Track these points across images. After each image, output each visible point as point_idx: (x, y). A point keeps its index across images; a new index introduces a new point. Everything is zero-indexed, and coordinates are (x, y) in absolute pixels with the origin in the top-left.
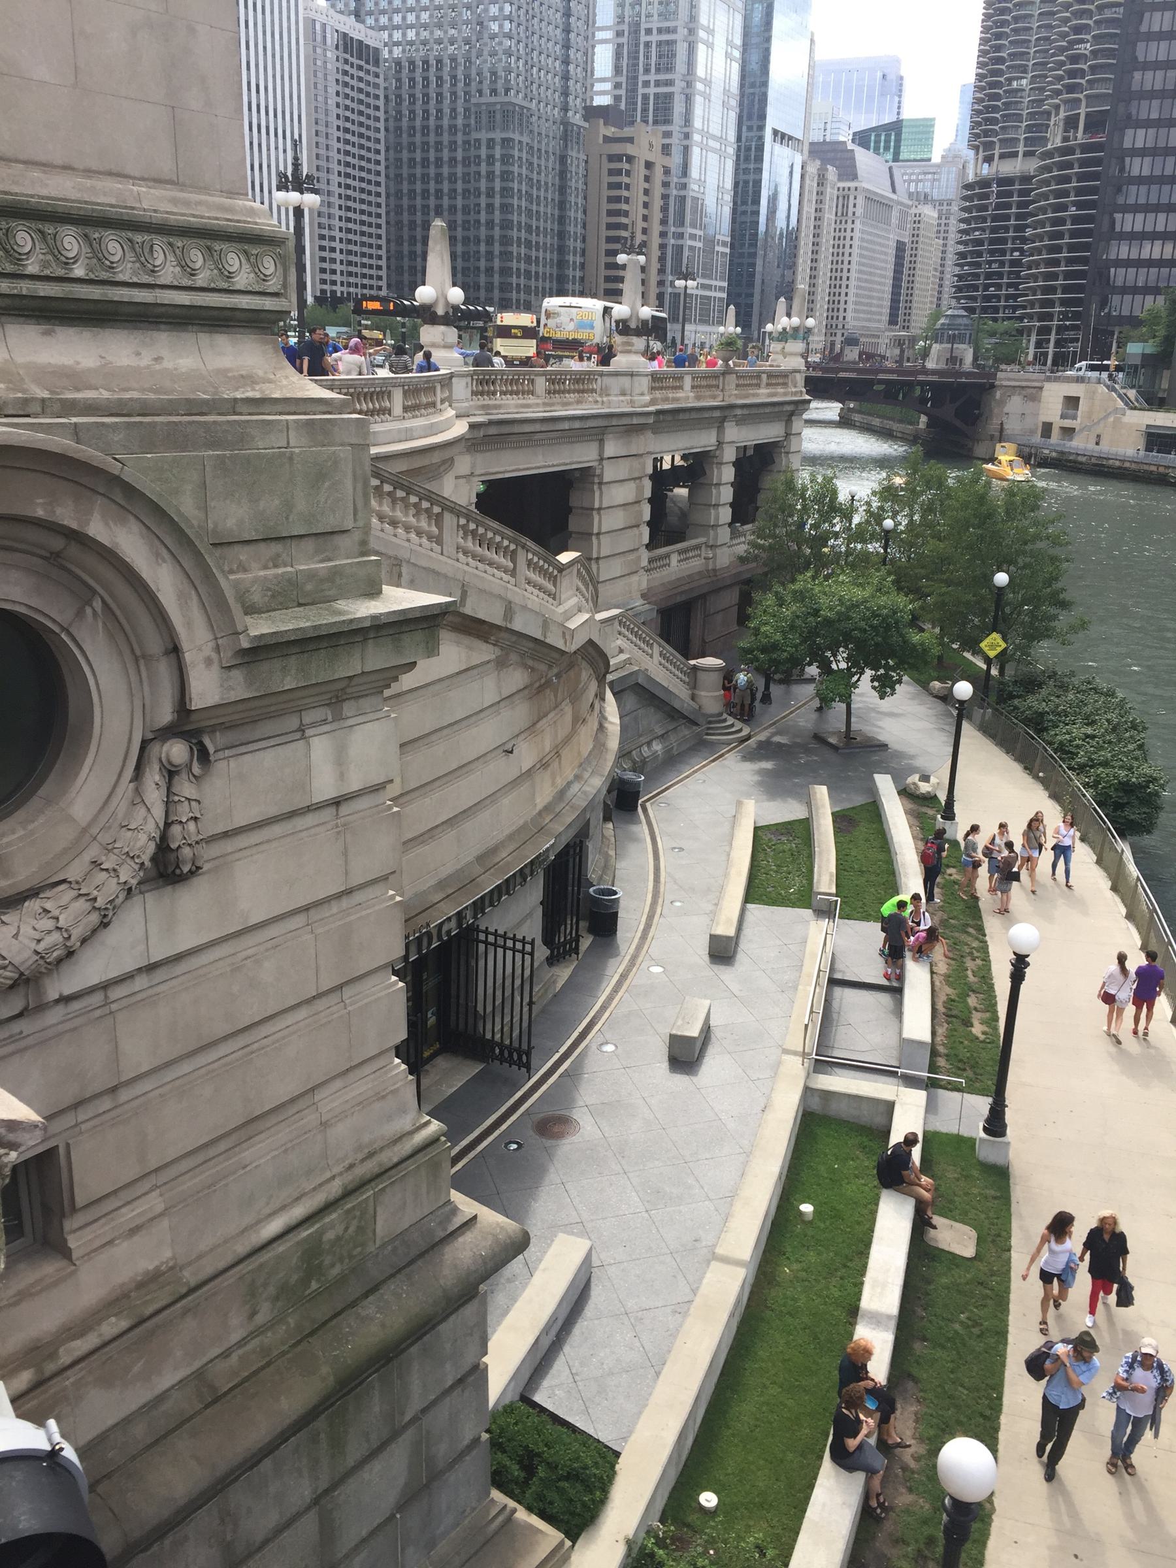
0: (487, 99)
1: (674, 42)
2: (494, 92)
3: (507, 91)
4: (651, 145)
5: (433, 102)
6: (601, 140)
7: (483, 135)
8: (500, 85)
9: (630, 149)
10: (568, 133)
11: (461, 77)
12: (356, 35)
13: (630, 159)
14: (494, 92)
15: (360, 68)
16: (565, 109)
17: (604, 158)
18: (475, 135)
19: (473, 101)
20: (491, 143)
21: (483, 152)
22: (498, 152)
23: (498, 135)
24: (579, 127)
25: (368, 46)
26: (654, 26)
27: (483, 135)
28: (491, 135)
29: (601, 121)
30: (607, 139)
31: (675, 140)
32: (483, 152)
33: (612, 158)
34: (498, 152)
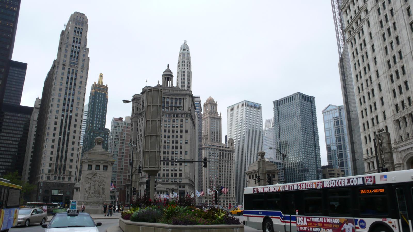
0: (301, 168)
1: (342, 153)
2: (302, 167)
3: (304, 167)
4: (338, 171)
5: (291, 170)
6: (328, 171)
7: (301, 174)
8: (303, 166)
9: (333, 172)
10: (318, 171)
11: (301, 165)
12: (278, 162)
13: (334, 174)
14: (302, 167)
15: (279, 166)
16: (317, 168)
17: (329, 174)
18: (300, 174)
19: (299, 169)
20: (302, 175)
21: (301, 176)
22: (303, 176)
23: (303, 174)
24: (320, 170)
25: (281, 163)
26: (338, 151)
27: (301, 174)
28: (302, 174)
29: (327, 168)
30: (329, 171)
31: (345, 169)
32: (301, 176)
33: (330, 174)
34: (303, 176)
